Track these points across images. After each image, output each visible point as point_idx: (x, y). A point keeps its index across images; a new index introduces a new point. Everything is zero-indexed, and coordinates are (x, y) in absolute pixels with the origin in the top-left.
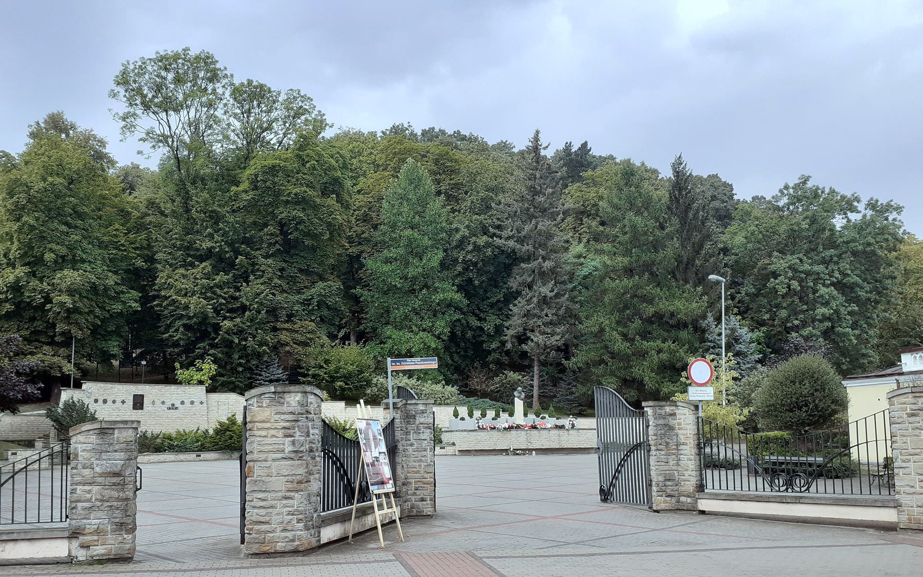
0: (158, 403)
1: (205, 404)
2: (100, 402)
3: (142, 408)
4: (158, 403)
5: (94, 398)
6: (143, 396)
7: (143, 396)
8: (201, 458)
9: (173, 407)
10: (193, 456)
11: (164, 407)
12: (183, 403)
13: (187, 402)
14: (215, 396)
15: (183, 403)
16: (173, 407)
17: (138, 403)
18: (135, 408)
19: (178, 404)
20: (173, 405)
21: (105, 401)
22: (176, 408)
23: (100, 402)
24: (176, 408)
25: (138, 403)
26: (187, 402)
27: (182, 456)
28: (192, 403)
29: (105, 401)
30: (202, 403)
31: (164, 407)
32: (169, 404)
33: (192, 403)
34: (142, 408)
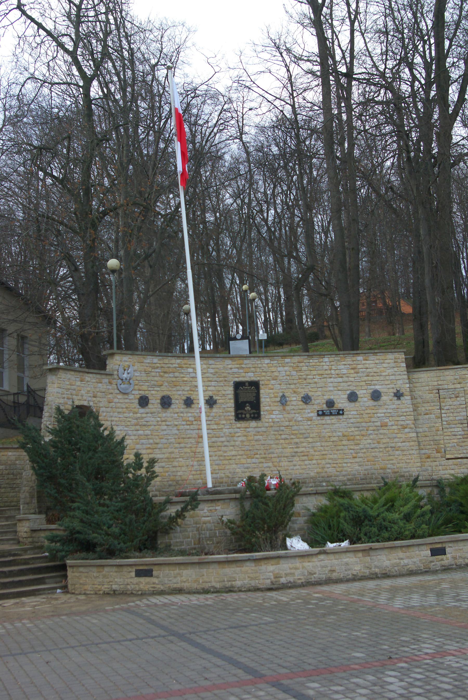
0: (295, 400)
1: (407, 399)
2: (155, 404)
3: (257, 416)
4: (295, 400)
5: (137, 394)
6: (255, 385)
7: (255, 385)
8: (447, 559)
9: (330, 410)
10: (416, 555)
11: (310, 411)
12: (353, 397)
13: (364, 394)
14: (428, 378)
15: (353, 397)
16: (330, 410)
17: (247, 401)
18: (239, 417)
19: (341, 402)
20: (330, 404)
21: (166, 402)
22: (340, 412)
23: (155, 404)
24: (340, 412)
25: (247, 401)
26: (364, 394)
27: (387, 558)
28: (376, 396)
29: (166, 402)
30: (398, 395)
31: (310, 411)
32: (319, 402)
33: (376, 396)
34: (257, 416)
